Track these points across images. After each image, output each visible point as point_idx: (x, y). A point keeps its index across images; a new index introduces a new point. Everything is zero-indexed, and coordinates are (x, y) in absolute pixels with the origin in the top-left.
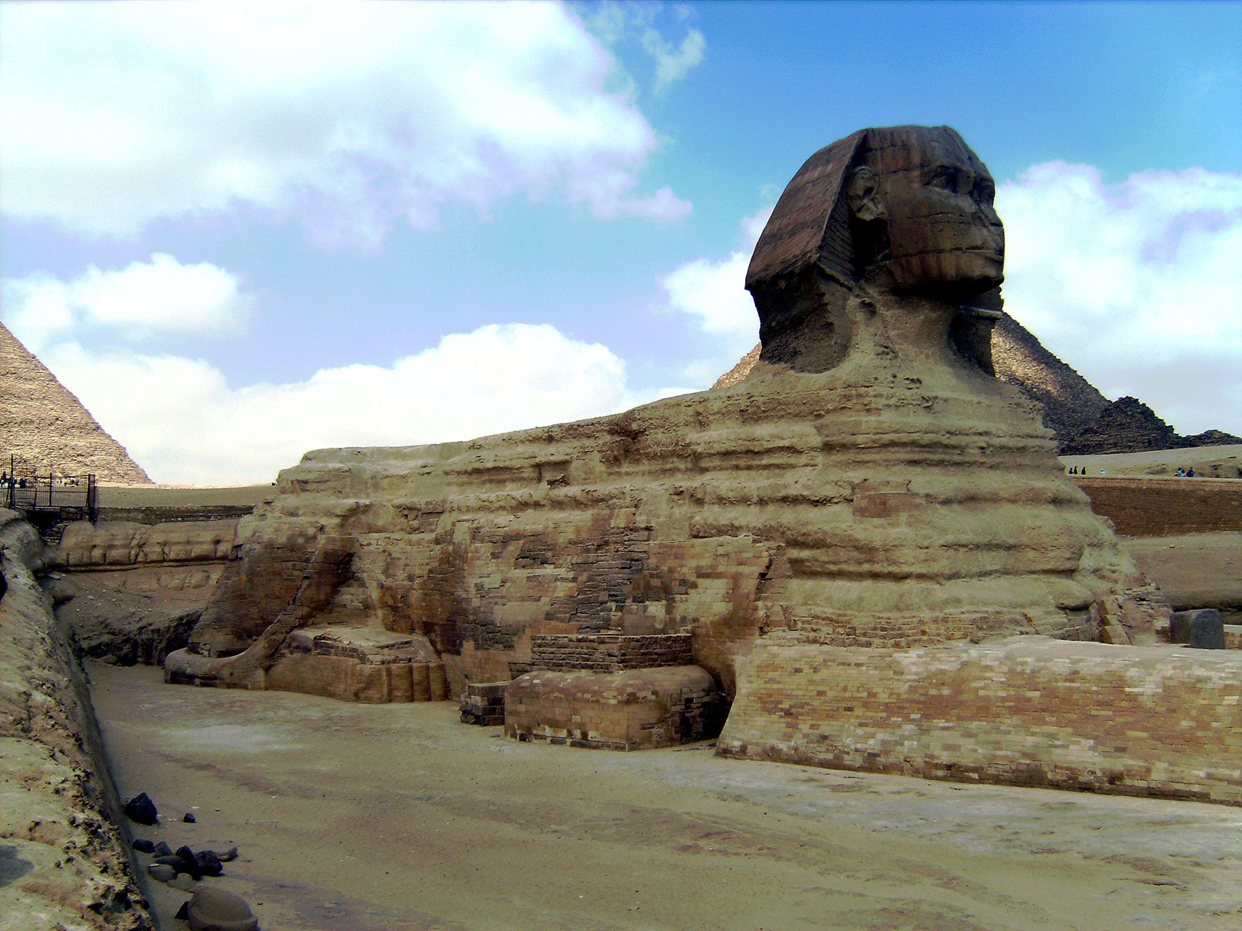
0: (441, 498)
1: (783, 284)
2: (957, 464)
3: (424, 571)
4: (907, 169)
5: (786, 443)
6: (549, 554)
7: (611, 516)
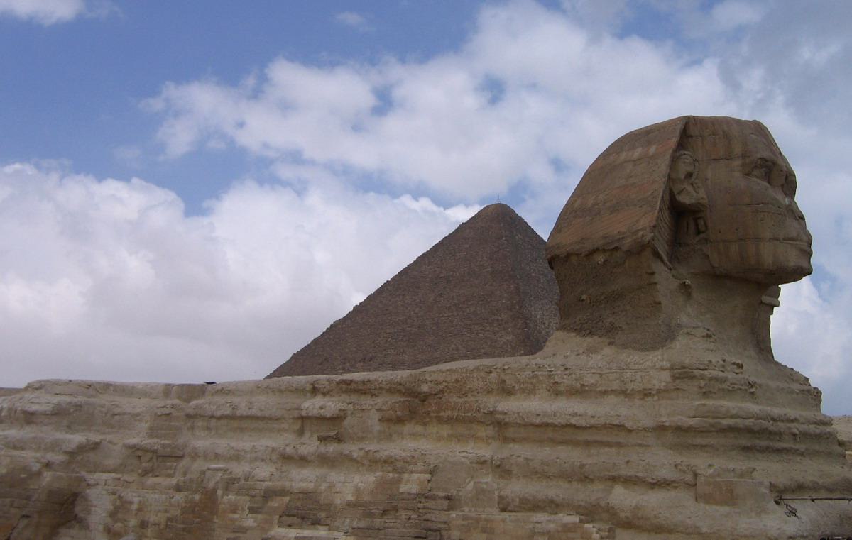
0: (181, 441)
1: (600, 258)
2: (779, 451)
3: (162, 518)
4: (728, 158)
5: (616, 422)
6: (323, 515)
7: (399, 481)
